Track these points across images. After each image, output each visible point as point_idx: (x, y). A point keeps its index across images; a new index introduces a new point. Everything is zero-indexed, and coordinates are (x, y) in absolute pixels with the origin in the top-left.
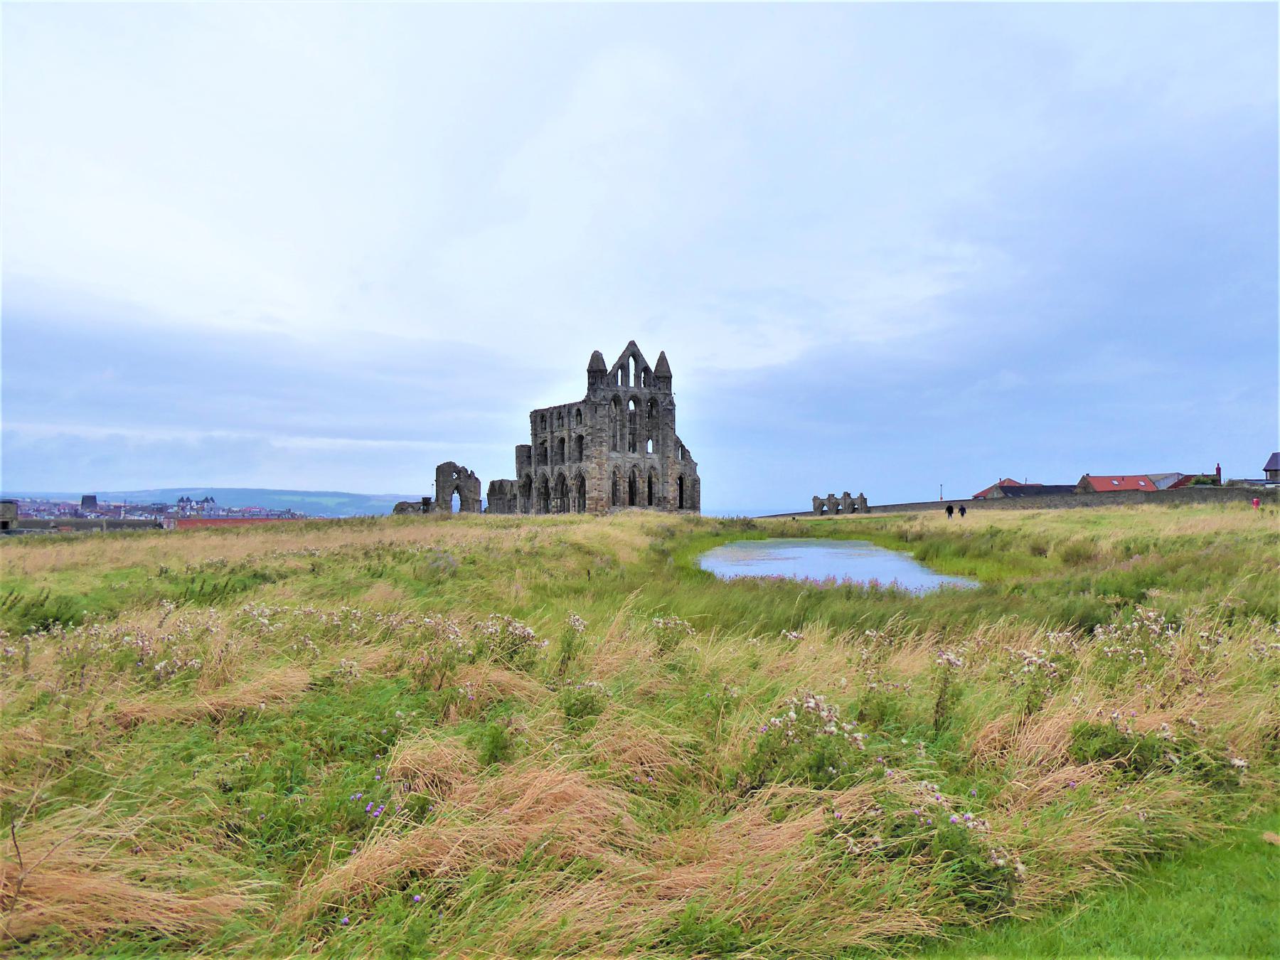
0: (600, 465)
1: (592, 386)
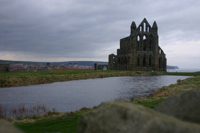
0: (133, 55)
1: (132, 32)
